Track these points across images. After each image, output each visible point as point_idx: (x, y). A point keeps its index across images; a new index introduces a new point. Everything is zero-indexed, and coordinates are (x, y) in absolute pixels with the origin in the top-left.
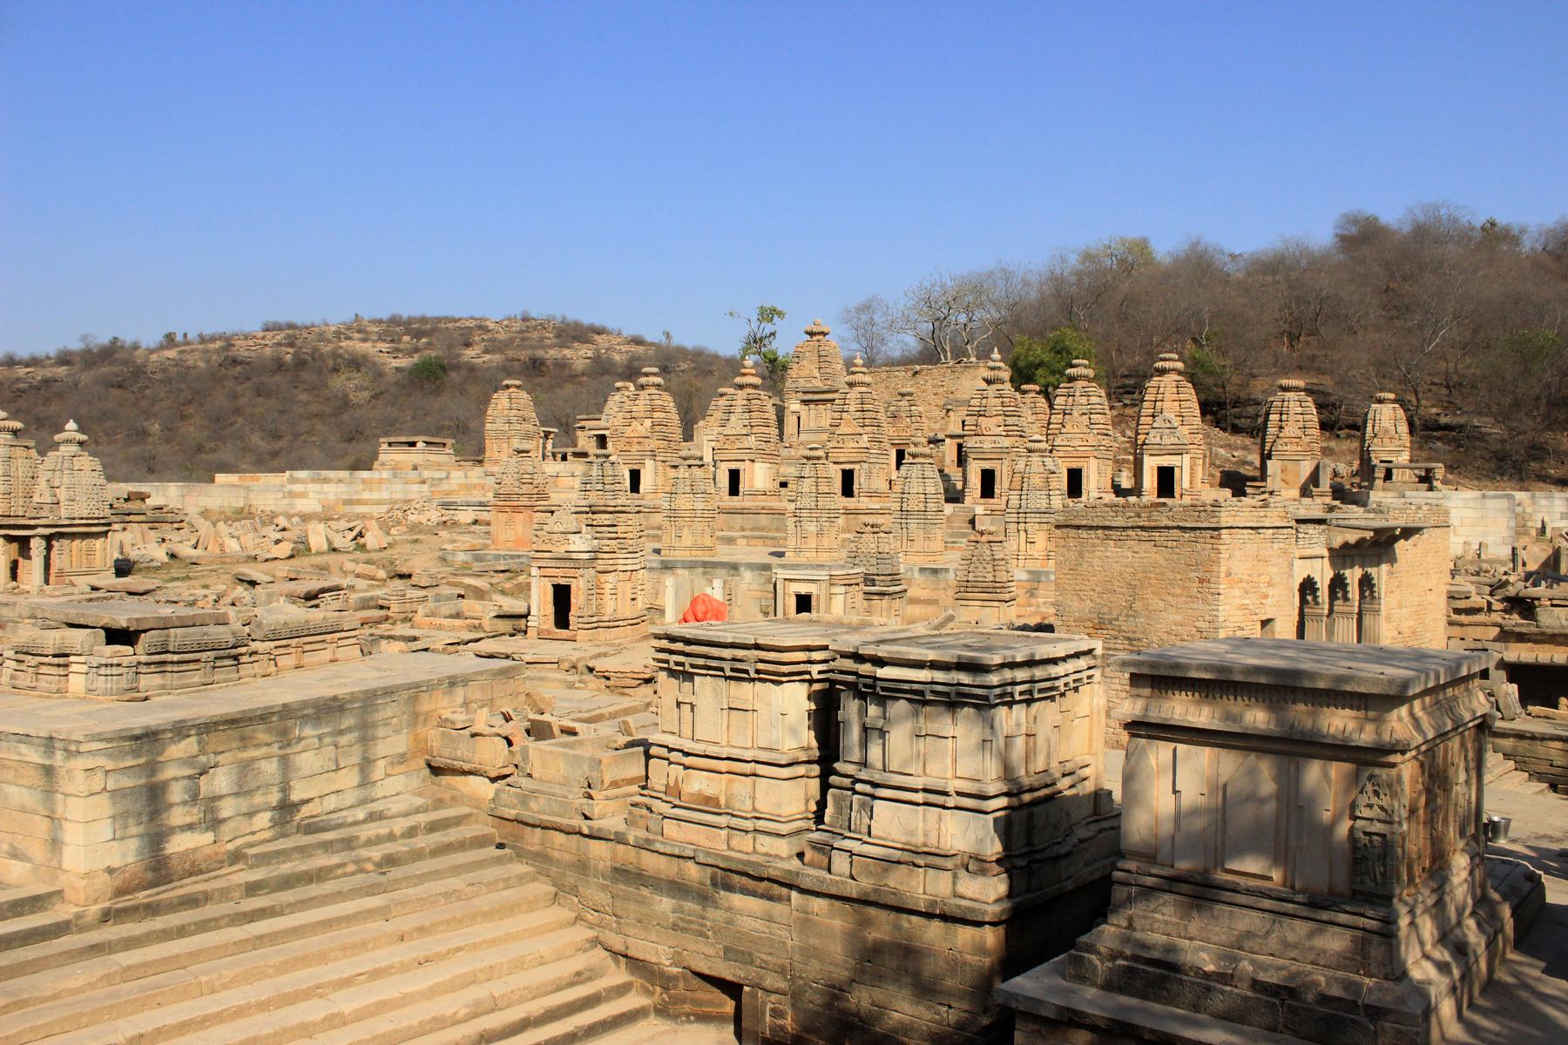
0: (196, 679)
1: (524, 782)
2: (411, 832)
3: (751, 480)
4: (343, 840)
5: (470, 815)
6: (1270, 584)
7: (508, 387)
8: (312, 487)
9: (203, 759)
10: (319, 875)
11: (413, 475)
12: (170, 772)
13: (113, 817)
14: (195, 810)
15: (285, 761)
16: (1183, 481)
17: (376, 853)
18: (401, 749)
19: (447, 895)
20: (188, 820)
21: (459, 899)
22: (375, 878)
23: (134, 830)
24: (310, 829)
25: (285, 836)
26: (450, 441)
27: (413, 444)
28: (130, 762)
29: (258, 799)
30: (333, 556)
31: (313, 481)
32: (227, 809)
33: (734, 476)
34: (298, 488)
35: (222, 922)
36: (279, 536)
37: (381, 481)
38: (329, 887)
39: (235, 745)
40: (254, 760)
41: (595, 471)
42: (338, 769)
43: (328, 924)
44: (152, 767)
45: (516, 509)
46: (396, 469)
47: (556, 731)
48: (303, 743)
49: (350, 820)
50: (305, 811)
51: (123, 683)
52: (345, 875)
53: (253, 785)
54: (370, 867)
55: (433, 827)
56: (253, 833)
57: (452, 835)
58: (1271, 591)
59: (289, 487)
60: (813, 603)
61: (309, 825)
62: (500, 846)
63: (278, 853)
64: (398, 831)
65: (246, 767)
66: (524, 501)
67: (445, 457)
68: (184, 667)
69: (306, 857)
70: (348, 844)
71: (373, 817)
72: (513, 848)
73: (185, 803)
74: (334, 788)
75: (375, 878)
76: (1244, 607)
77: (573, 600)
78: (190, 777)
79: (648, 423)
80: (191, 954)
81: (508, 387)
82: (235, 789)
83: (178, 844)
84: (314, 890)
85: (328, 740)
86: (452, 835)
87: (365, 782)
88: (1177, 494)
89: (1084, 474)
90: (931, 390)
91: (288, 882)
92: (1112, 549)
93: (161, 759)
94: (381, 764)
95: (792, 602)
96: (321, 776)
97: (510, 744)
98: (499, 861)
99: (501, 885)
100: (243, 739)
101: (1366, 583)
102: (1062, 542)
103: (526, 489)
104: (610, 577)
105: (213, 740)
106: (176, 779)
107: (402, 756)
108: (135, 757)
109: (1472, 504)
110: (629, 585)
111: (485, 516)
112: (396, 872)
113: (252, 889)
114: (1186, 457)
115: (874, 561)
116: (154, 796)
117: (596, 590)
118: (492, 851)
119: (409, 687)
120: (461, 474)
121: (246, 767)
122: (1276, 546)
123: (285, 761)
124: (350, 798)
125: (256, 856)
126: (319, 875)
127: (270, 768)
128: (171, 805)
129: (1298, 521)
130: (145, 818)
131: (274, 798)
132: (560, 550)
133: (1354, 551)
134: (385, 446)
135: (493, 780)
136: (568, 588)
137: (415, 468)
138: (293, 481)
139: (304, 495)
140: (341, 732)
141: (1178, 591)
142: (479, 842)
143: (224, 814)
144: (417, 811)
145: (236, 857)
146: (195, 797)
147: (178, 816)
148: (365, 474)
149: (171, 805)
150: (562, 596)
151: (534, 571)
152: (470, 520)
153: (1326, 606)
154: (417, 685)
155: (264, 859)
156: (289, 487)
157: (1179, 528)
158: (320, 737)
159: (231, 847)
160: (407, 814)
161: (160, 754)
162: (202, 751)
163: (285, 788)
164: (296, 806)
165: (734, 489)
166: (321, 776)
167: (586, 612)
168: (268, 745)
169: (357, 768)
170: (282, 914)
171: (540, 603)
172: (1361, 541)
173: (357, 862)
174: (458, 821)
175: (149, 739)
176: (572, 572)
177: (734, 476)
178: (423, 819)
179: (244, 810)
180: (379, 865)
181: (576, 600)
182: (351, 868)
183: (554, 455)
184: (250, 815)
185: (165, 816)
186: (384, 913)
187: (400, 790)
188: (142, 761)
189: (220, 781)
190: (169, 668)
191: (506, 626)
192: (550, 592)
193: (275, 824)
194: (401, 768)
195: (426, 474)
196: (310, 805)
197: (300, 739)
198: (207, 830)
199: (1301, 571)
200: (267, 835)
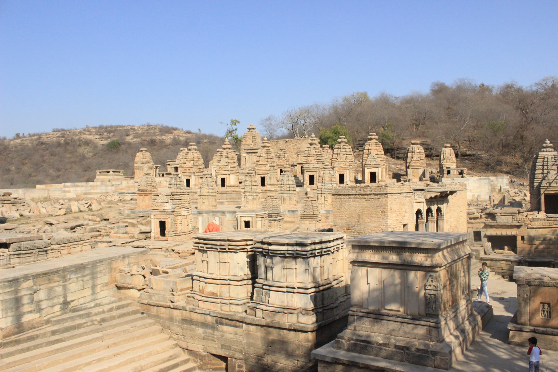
0: (32, 260)
1: (150, 291)
2: (111, 310)
4: (86, 314)
5: (131, 303)
6: (405, 212)
9: (35, 287)
10: (79, 326)
11: (109, 183)
12: (23, 293)
13: (2, 310)
14: (32, 306)
15: (65, 287)
17: (98, 318)
18: (106, 281)
19: (124, 331)
20: (30, 309)
21: (128, 332)
22: (98, 327)
23: (10, 314)
24: (74, 310)
25: (65, 313)
26: (122, 171)
27: (108, 172)
28: (8, 290)
29: (55, 301)
30: (81, 214)
31: (72, 186)
32: (44, 305)
34: (67, 189)
35: (43, 345)
36: (60, 207)
37: (97, 186)
38: (82, 330)
39: (46, 282)
40: (53, 287)
41: (173, 180)
42: (84, 289)
43: (82, 343)
44: (16, 291)
45: (146, 195)
46: (102, 181)
47: (161, 272)
48: (71, 280)
49: (89, 307)
50: (72, 304)
51: (5, 262)
52: (87, 326)
53: (53, 296)
54: (96, 323)
55: (118, 308)
56: (54, 313)
57: (125, 310)
58: (406, 214)
59: (64, 189)
60: (251, 224)
61: (74, 309)
62: (142, 313)
63: (63, 320)
64: (106, 309)
65: (50, 290)
66: (149, 192)
67: (120, 176)
68: (27, 255)
69: (73, 320)
70: (88, 315)
71: (97, 305)
72: (146, 314)
73: (29, 303)
74: (83, 296)
75: (98, 327)
77: (166, 226)
78: (30, 294)
80: (32, 357)
82: (47, 298)
83: (26, 319)
84: (76, 332)
85: (80, 279)
86: (125, 310)
87: (94, 293)
91: (67, 330)
93: (20, 288)
94: (99, 286)
95: (243, 224)
96: (78, 291)
97: (145, 277)
98: (142, 319)
99: (143, 327)
100: (49, 280)
102: (335, 200)
103: (149, 187)
104: (179, 218)
105: (39, 281)
106: (25, 295)
107: (107, 283)
108: (10, 288)
110: (186, 220)
111: (135, 197)
112: (105, 324)
113: (54, 333)
115: (271, 209)
116: (18, 301)
117: (174, 222)
118: (140, 315)
119: (108, 259)
120: (126, 182)
121: (50, 290)
123: (65, 287)
124: (88, 299)
125: (55, 321)
126: (79, 326)
127: (59, 290)
128: (23, 305)
129: (414, 190)
130: (14, 310)
131: (61, 300)
132: (161, 209)
134: (98, 173)
135: (139, 290)
136: (164, 222)
137: (109, 181)
138: (65, 187)
140: (85, 276)
142: (135, 312)
143: (43, 307)
144: (113, 303)
145: (48, 322)
146: (32, 301)
147: (26, 308)
148: (91, 183)
149: (23, 305)
150: (162, 225)
151: (152, 217)
152: (129, 199)
153: (425, 219)
154: (111, 258)
155: (58, 322)
156: (64, 189)
158: (77, 278)
159: (46, 318)
160: (109, 304)
161: (19, 286)
162: (35, 285)
163: (65, 296)
164: (69, 303)
166: (78, 291)
167: (171, 230)
168: (58, 281)
169: (91, 289)
170: (65, 341)
172: (436, 196)
173: (92, 321)
174: (127, 305)
175: (15, 281)
176: (166, 216)
178: (115, 305)
179: (50, 305)
180: (99, 322)
181: (168, 226)
182: (89, 323)
184: (53, 306)
185: (21, 308)
186: (102, 339)
187: (106, 295)
188: (13, 289)
189: (41, 295)
190: (22, 256)
191: (143, 236)
192: (158, 223)
193: (62, 309)
194: (107, 287)
195: (113, 183)
196: (74, 302)
197: (70, 279)
198: (37, 312)
199: (416, 207)
200: (59, 313)
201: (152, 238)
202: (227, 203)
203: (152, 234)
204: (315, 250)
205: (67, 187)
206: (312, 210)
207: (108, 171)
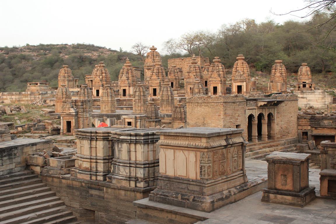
3: (129, 92)
6: (239, 116)
7: (64, 67)
8: (8, 97)
16: (244, 89)
27: (37, 84)
33: (124, 91)
60: (132, 124)
76: (230, 122)
79: (101, 77)
81: (64, 67)
88: (242, 93)
89: (218, 88)
90: (186, 65)
92: (199, 108)
101: (270, 116)
109: (321, 94)
114: (245, 83)
122: (240, 106)
132: (68, 112)
133: (265, 107)
134: (29, 85)
139: (6, 99)
141: (214, 118)
150: (69, 123)
152: (52, 104)
157: (213, 102)
165: (124, 94)
171: (63, 127)
172: (265, 105)
177: (124, 91)
183: (77, 86)
191: (54, 132)
201: (61, 134)
202: (125, 109)
203: (61, 131)
204: (149, 139)
205: (4, 95)
206: (180, 114)
207: (36, 83)
